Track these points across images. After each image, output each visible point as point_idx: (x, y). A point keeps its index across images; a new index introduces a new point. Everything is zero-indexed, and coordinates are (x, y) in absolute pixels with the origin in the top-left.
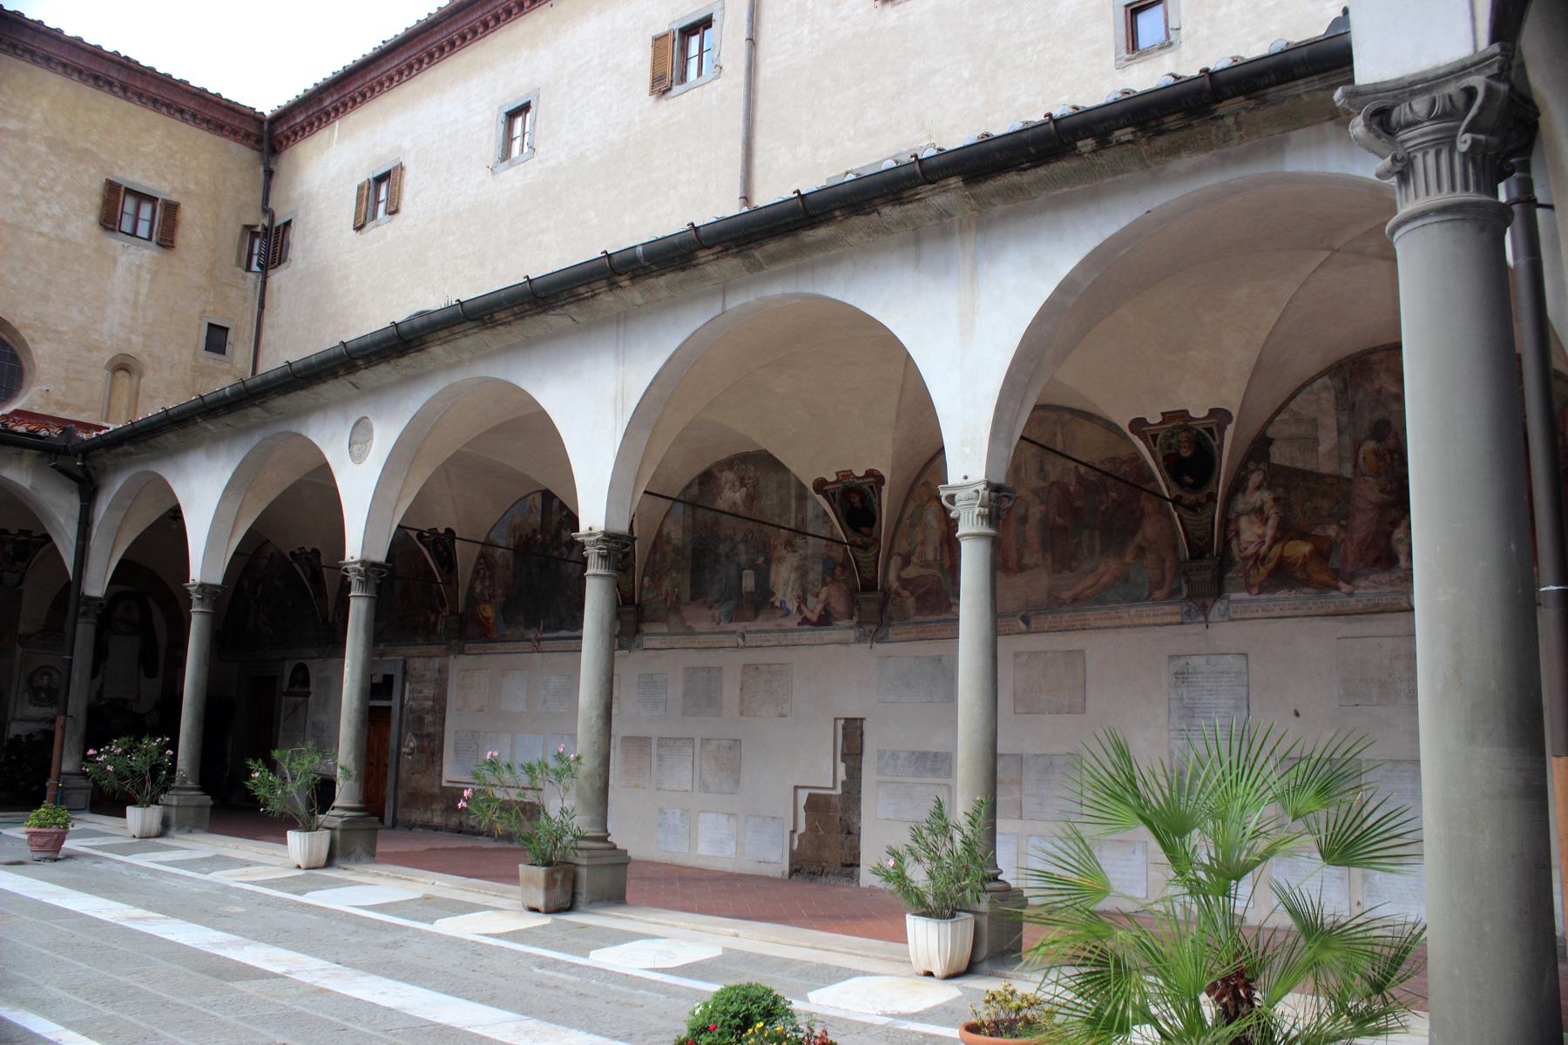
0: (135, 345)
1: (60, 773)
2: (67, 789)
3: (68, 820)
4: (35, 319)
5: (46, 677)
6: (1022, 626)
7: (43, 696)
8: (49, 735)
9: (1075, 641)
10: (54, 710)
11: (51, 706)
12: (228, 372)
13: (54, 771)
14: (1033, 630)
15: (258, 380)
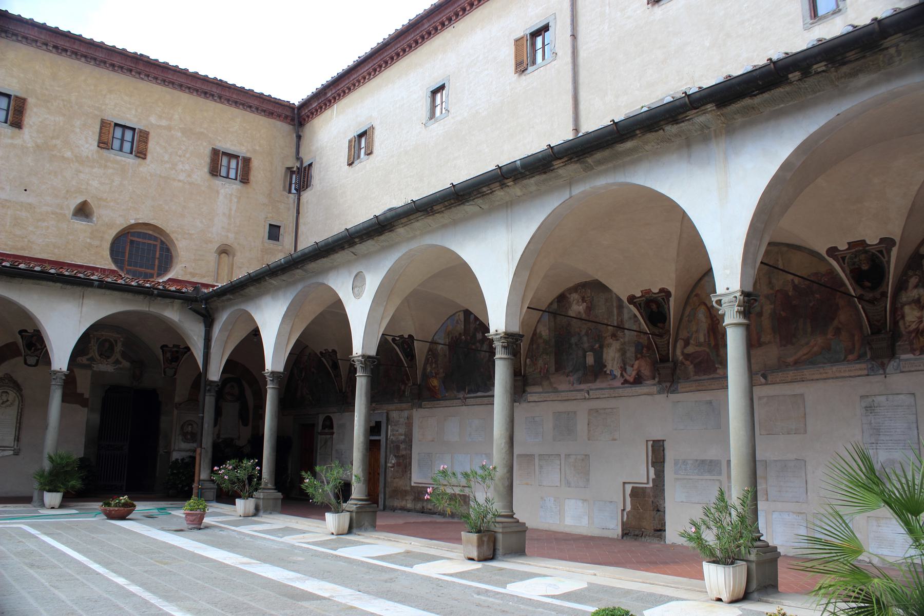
0: (230, 239)
1: (200, 480)
2: (203, 489)
3: (205, 507)
4: (178, 228)
5: (190, 426)
6: (763, 380)
7: (189, 437)
8: (193, 458)
9: (797, 389)
10: (195, 445)
11: (193, 442)
12: (281, 251)
13: (196, 479)
14: (769, 382)
15: (299, 254)
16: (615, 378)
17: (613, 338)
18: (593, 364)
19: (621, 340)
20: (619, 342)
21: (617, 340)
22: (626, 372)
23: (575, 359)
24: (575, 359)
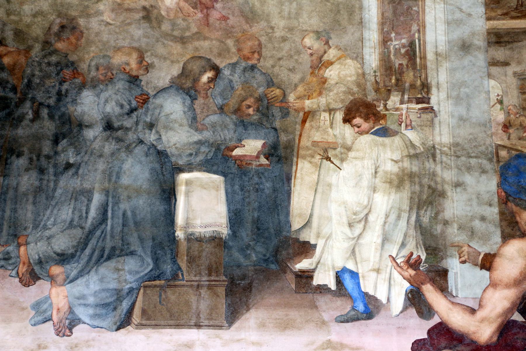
16: (369, 315)
17: (358, 121)
18: (225, 231)
19: (411, 135)
20: (397, 140)
21: (384, 132)
22: (443, 289)
23: (97, 199)
24: (97, 199)
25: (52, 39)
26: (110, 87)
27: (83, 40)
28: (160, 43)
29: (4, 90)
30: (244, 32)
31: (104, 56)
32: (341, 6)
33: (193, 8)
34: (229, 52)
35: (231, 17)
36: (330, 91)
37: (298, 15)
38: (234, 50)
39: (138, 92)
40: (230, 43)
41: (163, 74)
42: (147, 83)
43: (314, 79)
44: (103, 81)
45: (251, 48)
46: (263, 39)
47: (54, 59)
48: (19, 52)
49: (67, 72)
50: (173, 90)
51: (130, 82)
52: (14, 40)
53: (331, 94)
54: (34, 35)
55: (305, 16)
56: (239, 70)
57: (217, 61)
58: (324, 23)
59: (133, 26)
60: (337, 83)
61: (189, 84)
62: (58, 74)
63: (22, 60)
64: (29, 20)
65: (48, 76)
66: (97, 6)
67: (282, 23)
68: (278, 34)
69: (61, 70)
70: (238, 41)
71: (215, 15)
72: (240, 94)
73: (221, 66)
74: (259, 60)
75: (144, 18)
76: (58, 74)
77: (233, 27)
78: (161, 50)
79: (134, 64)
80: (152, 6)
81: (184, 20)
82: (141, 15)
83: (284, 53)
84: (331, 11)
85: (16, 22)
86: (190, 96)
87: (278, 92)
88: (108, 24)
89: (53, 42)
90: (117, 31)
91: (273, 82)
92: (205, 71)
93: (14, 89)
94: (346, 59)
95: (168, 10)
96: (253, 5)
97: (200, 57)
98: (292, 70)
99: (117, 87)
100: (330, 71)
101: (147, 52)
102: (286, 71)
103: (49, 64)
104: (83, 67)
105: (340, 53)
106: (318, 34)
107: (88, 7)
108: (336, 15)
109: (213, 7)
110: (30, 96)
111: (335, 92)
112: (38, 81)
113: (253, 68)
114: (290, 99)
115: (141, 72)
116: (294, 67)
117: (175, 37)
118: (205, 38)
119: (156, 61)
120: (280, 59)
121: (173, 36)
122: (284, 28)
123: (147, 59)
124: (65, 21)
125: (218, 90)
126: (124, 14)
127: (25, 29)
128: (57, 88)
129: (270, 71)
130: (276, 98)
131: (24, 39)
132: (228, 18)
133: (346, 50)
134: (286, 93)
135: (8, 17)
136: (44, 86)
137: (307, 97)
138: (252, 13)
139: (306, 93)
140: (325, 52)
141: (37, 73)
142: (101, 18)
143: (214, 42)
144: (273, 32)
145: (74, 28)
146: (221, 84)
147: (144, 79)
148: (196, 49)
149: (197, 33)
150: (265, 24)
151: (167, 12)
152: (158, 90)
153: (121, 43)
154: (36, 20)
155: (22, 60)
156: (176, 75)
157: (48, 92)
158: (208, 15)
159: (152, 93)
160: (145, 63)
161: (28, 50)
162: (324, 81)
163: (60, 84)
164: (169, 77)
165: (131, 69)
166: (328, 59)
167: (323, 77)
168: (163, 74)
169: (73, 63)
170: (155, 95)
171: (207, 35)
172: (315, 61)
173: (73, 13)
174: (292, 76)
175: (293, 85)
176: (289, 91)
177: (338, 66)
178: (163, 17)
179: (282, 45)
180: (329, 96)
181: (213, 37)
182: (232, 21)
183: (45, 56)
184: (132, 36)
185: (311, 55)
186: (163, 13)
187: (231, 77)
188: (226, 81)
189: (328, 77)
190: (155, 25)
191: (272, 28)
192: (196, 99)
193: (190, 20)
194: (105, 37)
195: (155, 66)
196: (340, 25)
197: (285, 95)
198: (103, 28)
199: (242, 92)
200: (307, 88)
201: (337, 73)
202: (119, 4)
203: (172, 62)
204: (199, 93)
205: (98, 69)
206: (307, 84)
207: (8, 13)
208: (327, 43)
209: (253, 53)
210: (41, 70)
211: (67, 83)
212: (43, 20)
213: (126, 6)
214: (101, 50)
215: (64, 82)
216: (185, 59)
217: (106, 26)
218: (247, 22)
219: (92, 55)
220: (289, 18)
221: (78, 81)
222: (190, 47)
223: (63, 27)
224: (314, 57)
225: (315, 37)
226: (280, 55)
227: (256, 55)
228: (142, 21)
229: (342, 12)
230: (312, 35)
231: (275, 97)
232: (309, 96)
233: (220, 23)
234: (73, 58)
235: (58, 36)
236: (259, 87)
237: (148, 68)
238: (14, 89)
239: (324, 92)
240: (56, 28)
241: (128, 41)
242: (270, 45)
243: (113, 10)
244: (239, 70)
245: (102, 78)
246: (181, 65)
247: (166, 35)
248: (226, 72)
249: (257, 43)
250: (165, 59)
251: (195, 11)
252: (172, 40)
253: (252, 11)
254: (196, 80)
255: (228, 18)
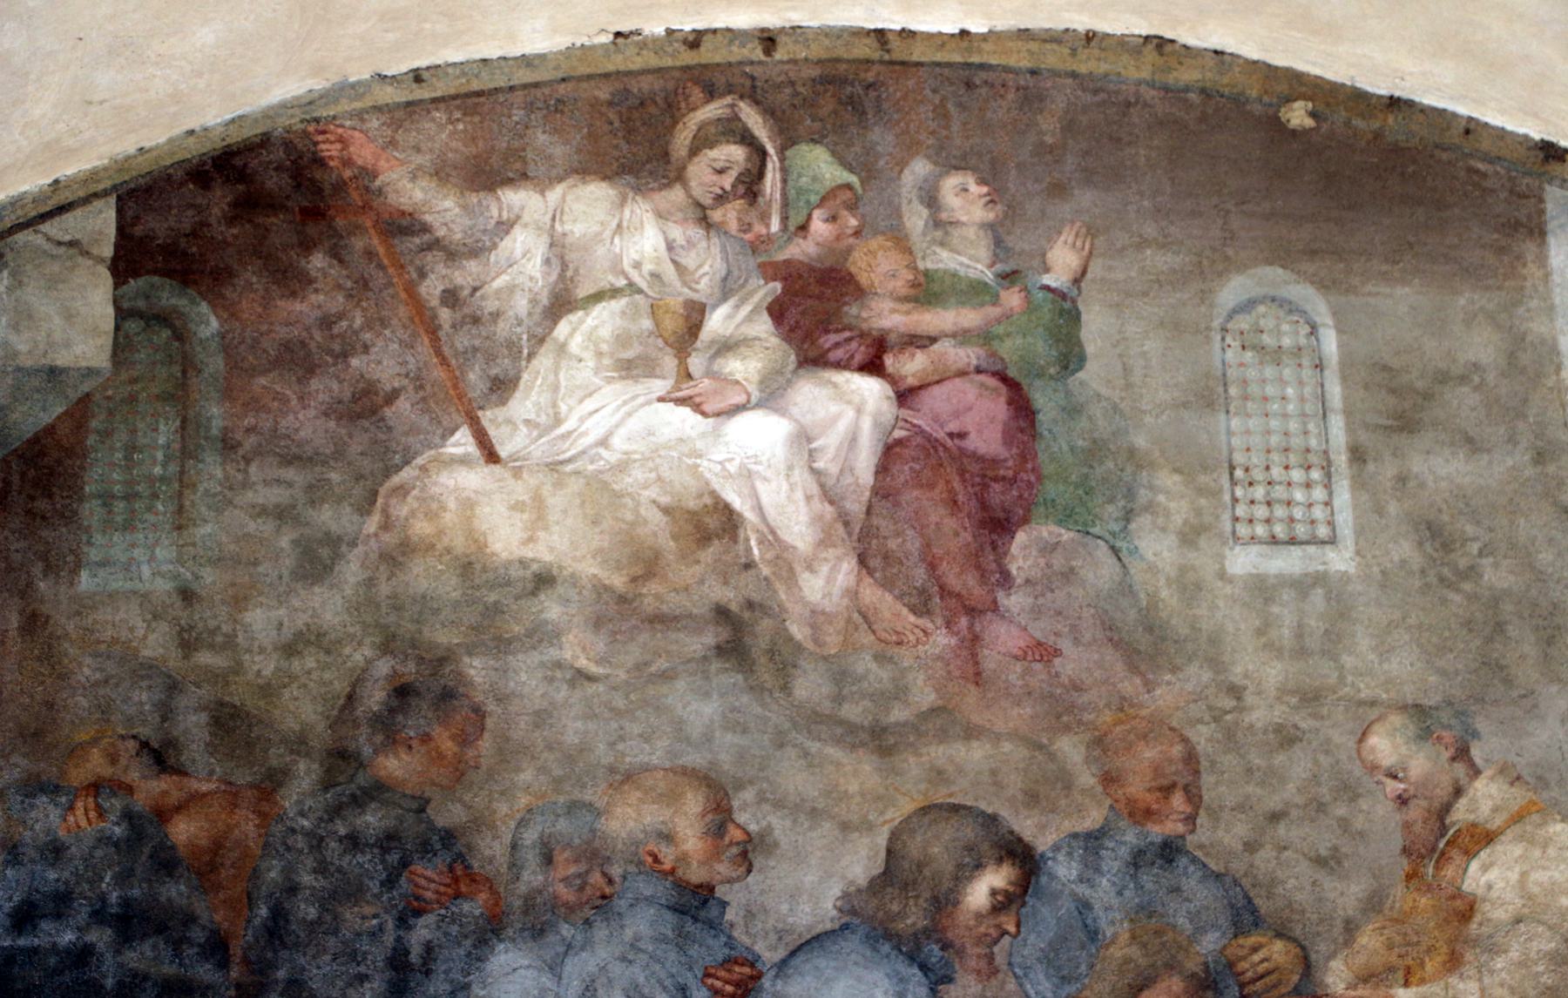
25: (363, 741)
26: (600, 932)
27: (486, 744)
28: (791, 752)
29: (177, 953)
30: (1123, 705)
31: (573, 807)
32: (1508, 607)
33: (914, 610)
34: (1068, 787)
35: (1065, 645)
36: (1495, 950)
37: (1334, 640)
38: (1087, 778)
39: (711, 951)
40: (1071, 749)
41: (810, 878)
42: (750, 915)
43: (1424, 901)
44: (571, 909)
45: (1157, 770)
46: (1203, 737)
47: (372, 820)
48: (232, 796)
49: (428, 874)
50: (852, 944)
51: (678, 910)
52: (212, 749)
53: (1499, 963)
54: (291, 725)
55: (1364, 643)
56: (1113, 862)
57: (1025, 826)
58: (1443, 672)
59: (681, 685)
60: (1518, 921)
61: (914, 918)
62: (390, 883)
63: (247, 826)
64: (266, 666)
65: (352, 892)
66: (533, 605)
67: (1274, 673)
68: (1260, 715)
69: (405, 864)
70: (1099, 742)
71: (1002, 638)
72: (1127, 960)
73: (1043, 843)
74: (1191, 819)
75: (721, 651)
76: (390, 883)
77: (1077, 687)
78: (795, 779)
79: (692, 838)
80: (750, 605)
81: (880, 658)
82: (709, 638)
83: (1290, 792)
84: (1468, 624)
85: (220, 678)
86: (924, 968)
87: (1278, 951)
88: (583, 676)
89: (367, 751)
90: (620, 703)
91: (1254, 911)
92: (979, 866)
93: (217, 948)
94: (1544, 823)
95: (817, 618)
96: (1153, 598)
97: (955, 809)
98: (1327, 862)
99: (629, 933)
100: (1485, 868)
101: (740, 786)
102: (1304, 867)
103: (354, 842)
104: (491, 850)
105: (1517, 797)
106: (1423, 720)
107: (496, 609)
108: (1489, 640)
109: (995, 607)
110: (281, 974)
111: (1514, 954)
112: (312, 913)
113: (1169, 851)
114: (1330, 980)
115: (723, 869)
116: (1335, 849)
117: (851, 728)
118: (971, 733)
119: (779, 824)
120: (1275, 817)
121: (841, 722)
122: (1283, 692)
123: (742, 817)
124: (411, 667)
125: (1034, 943)
126: (644, 637)
127: (253, 704)
128: (389, 939)
129: (1239, 867)
130: (1273, 977)
131: (250, 745)
132: (1057, 653)
133: (1542, 782)
134: (1313, 957)
135: (186, 657)
136: (336, 932)
137: (1400, 974)
138: (1150, 629)
139: (1393, 958)
140: (1458, 792)
141: (307, 879)
142: (553, 653)
143: (1007, 747)
144: (1240, 709)
145: (447, 695)
146: (1046, 919)
147: (735, 897)
148: (938, 775)
149: (934, 711)
150: (1206, 676)
151: (814, 627)
152: (793, 941)
153: (636, 754)
154: (296, 665)
155: (247, 826)
156: (862, 881)
157: (354, 956)
158: (974, 640)
159: (769, 954)
160: (734, 834)
161: (271, 785)
162: (1464, 910)
163: (403, 922)
164: (836, 891)
165: (683, 858)
166: (1472, 817)
167: (1458, 894)
168: (810, 878)
169: (448, 837)
170: (784, 963)
171: (976, 719)
172: (1418, 828)
173: (444, 637)
174: (1330, 885)
175: (1339, 923)
176: (1323, 947)
177: (1518, 850)
178: (799, 648)
179: (1280, 759)
180: (1492, 972)
181: (1000, 726)
182: (1073, 662)
183: (335, 811)
184: (679, 726)
185: (1402, 801)
186: (798, 631)
187: (1083, 890)
188: (1066, 906)
189: (1480, 892)
190: (766, 675)
191: (1236, 691)
192: (948, 979)
193: (906, 658)
194: (572, 729)
195: (776, 844)
196: (1508, 682)
197: (1307, 966)
198: (562, 693)
199: (1134, 952)
200: (1398, 939)
201: (1514, 876)
202: (622, 599)
203: (845, 827)
204: (961, 953)
205: (548, 860)
206: (1396, 921)
207: (188, 643)
208: (1462, 753)
209: (1167, 790)
210: (322, 869)
211: (430, 919)
212: (325, 667)
213: (649, 605)
214: (558, 783)
215: (419, 913)
216: (895, 815)
217: (572, 684)
218: (1133, 669)
219: (523, 801)
220: (1301, 652)
221: (473, 908)
222: (913, 766)
223: (403, 692)
224: (1415, 812)
225: (1412, 730)
226: (1274, 802)
227: (1178, 801)
228: (715, 666)
229: (1512, 631)
230: (1396, 719)
231: (1269, 973)
232: (1408, 971)
233: (1027, 672)
234: (448, 814)
235: (387, 726)
236: (1200, 930)
237: (748, 852)
238: (217, 948)
239: (1469, 956)
240: (375, 698)
241: (662, 744)
242: (1229, 760)
243: (598, 623)
244: (1113, 862)
245: (565, 893)
246: (882, 840)
247: (814, 720)
248: (1064, 870)
249: (1177, 750)
250: (814, 813)
251: (924, 622)
252: (838, 741)
253: (1151, 623)
254: (944, 902)
255: (1057, 653)
